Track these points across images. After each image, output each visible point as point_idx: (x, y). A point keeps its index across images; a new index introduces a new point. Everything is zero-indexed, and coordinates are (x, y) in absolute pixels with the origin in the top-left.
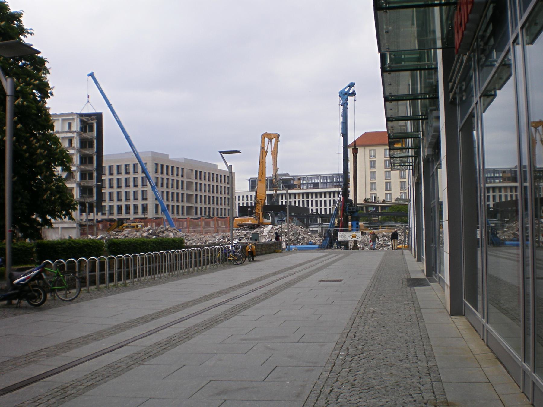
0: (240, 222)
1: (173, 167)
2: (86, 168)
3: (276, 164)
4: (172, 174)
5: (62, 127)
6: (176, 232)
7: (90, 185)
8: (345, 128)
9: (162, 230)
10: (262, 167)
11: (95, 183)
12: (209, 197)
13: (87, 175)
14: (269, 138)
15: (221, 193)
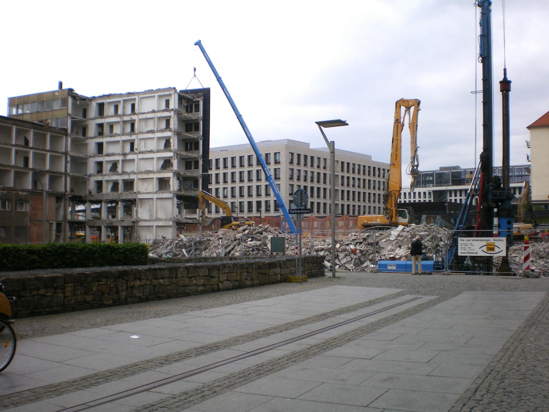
0: (366, 221)
1: (312, 158)
2: (188, 154)
3: (416, 141)
4: (312, 166)
5: (159, 104)
7: (194, 175)
8: (486, 47)
9: (260, 230)
10: (397, 147)
11: (201, 173)
12: (359, 193)
13: (193, 164)
14: (407, 106)
15: (374, 188)
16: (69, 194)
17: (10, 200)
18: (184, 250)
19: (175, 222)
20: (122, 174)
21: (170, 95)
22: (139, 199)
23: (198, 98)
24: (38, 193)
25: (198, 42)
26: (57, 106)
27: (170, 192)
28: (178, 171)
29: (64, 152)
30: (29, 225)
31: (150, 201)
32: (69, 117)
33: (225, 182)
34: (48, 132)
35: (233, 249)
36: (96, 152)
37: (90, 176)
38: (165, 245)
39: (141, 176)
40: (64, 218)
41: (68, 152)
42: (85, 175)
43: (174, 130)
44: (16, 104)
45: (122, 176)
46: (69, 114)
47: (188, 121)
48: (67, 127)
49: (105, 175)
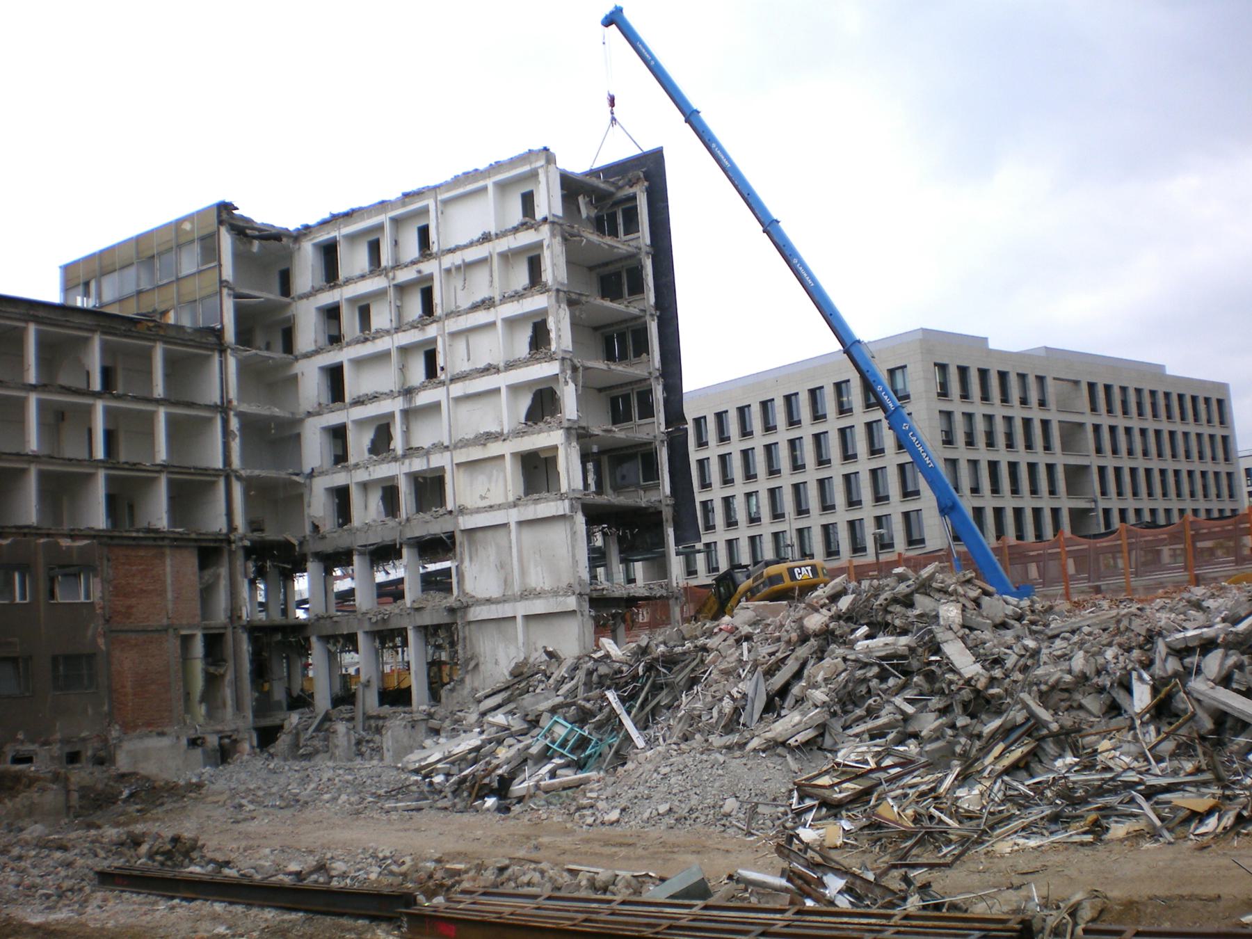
1: (1003, 376)
6: (974, 593)
9: (902, 588)
11: (663, 428)
16: (241, 539)
17: (25, 568)
18: (611, 695)
19: (587, 598)
20: (404, 456)
21: (533, 175)
22: (463, 531)
23: (631, 187)
24: (134, 538)
25: (612, 13)
26: (189, 263)
27: (562, 497)
28: (584, 424)
29: (219, 403)
30: (103, 647)
31: (500, 535)
32: (225, 291)
33: (750, 476)
34: (155, 341)
35: (798, 675)
36: (325, 397)
37: (312, 475)
38: (551, 681)
39: (463, 456)
40: (231, 618)
41: (230, 402)
42: (297, 475)
43: (554, 288)
44: (81, 281)
45: (407, 462)
46: (226, 281)
47: (606, 264)
48: (222, 323)
49: (357, 466)
